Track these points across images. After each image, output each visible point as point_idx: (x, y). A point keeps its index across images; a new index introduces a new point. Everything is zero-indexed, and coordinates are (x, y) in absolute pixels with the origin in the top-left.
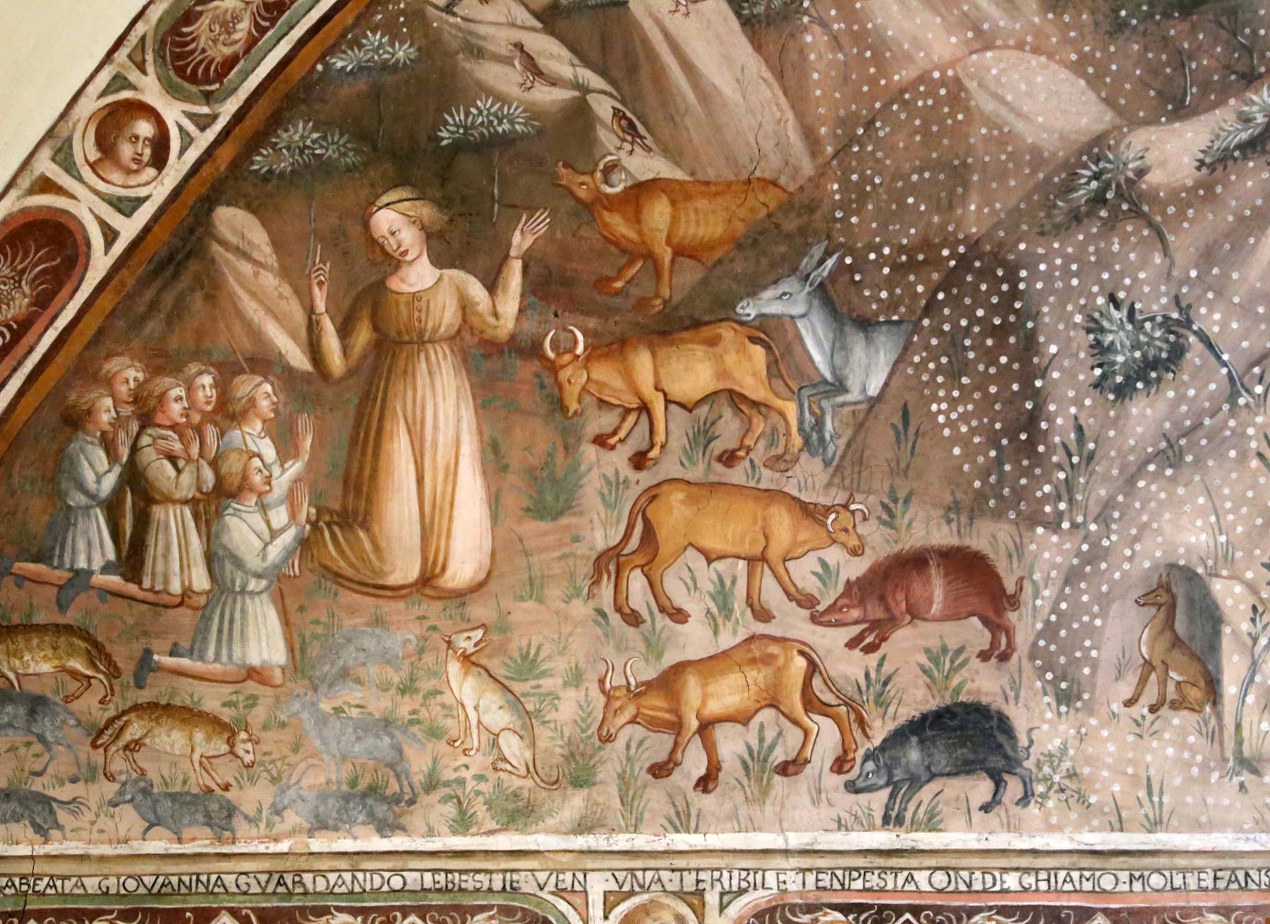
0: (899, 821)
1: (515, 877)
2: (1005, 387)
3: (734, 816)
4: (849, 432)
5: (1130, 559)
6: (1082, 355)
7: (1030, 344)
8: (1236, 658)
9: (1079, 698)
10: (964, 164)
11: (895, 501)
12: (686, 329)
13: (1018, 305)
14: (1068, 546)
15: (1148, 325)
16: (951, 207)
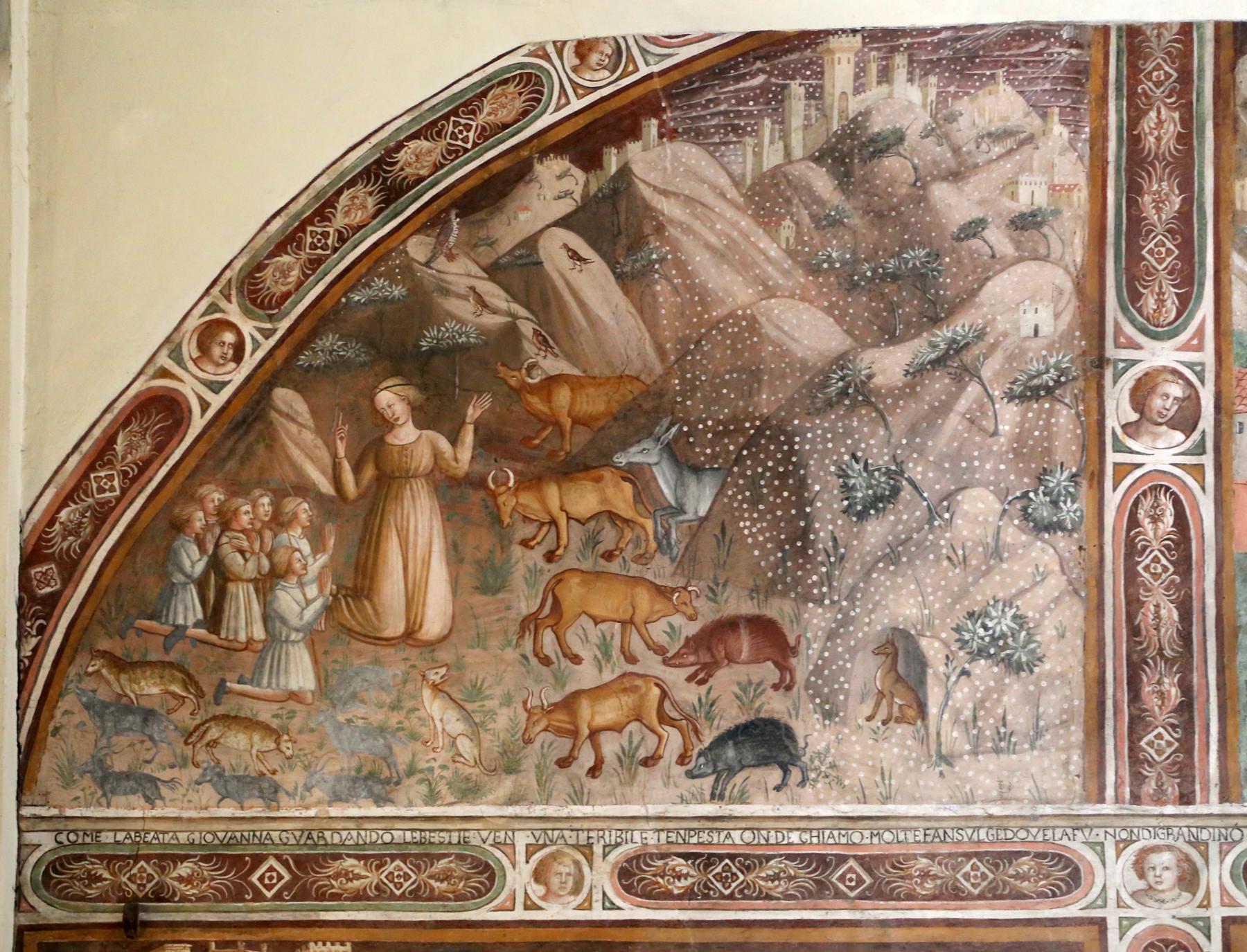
0: (721, 797)
1: (467, 834)
2: (787, 511)
3: (612, 794)
4: (687, 540)
5: (868, 624)
6: (835, 492)
7: (802, 484)
8: (936, 689)
9: (837, 715)
10: (758, 368)
11: (717, 585)
12: (580, 471)
13: (794, 459)
14: (829, 615)
15: (876, 474)
16: (750, 395)
